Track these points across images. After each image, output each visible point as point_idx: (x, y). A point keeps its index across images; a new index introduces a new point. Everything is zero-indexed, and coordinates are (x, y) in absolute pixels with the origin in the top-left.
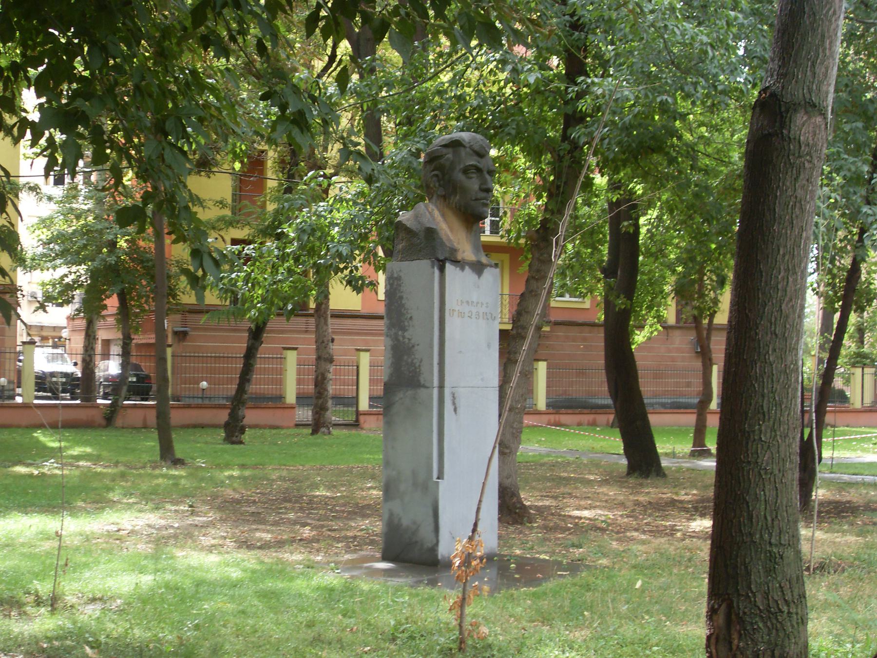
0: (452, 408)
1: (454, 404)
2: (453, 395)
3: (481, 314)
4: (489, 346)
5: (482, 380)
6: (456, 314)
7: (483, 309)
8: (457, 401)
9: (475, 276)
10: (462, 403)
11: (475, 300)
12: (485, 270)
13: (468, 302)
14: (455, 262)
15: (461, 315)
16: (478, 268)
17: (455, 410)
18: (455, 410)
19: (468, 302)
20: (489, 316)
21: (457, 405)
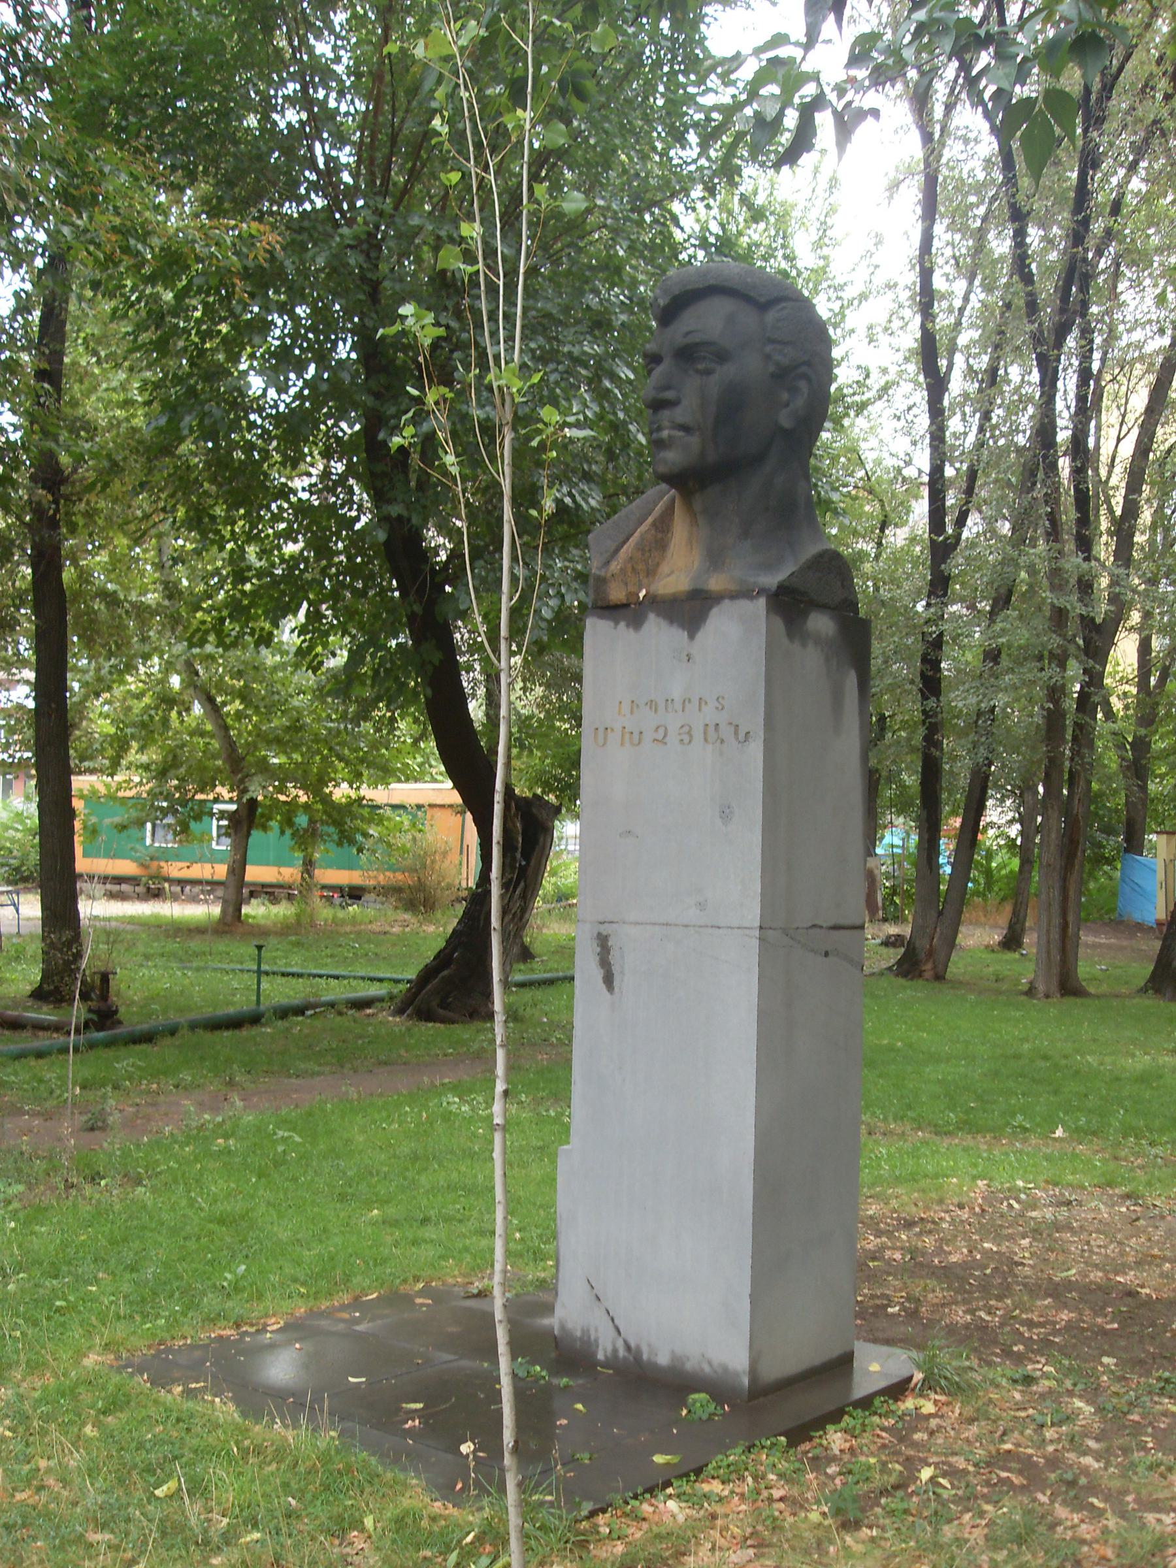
0: (598, 974)
1: (605, 962)
2: (603, 942)
3: (698, 734)
4: (726, 814)
5: (701, 906)
6: (613, 738)
7: (709, 714)
8: (614, 957)
9: (678, 635)
10: (626, 962)
11: (677, 693)
12: (715, 611)
13: (652, 704)
14: (611, 610)
15: (634, 738)
16: (690, 610)
17: (609, 980)
18: (609, 980)
19: (652, 704)
20: (727, 732)
21: (616, 969)
